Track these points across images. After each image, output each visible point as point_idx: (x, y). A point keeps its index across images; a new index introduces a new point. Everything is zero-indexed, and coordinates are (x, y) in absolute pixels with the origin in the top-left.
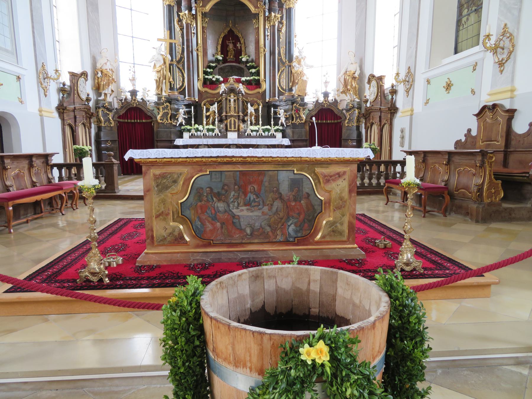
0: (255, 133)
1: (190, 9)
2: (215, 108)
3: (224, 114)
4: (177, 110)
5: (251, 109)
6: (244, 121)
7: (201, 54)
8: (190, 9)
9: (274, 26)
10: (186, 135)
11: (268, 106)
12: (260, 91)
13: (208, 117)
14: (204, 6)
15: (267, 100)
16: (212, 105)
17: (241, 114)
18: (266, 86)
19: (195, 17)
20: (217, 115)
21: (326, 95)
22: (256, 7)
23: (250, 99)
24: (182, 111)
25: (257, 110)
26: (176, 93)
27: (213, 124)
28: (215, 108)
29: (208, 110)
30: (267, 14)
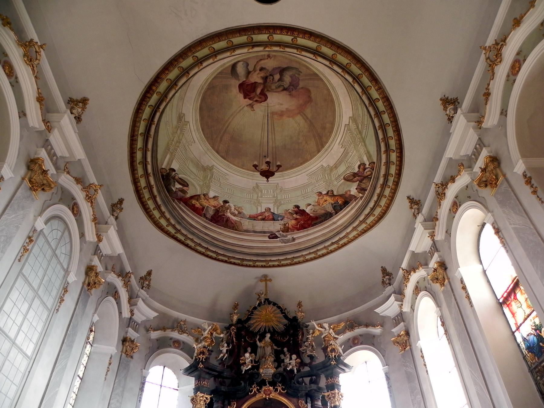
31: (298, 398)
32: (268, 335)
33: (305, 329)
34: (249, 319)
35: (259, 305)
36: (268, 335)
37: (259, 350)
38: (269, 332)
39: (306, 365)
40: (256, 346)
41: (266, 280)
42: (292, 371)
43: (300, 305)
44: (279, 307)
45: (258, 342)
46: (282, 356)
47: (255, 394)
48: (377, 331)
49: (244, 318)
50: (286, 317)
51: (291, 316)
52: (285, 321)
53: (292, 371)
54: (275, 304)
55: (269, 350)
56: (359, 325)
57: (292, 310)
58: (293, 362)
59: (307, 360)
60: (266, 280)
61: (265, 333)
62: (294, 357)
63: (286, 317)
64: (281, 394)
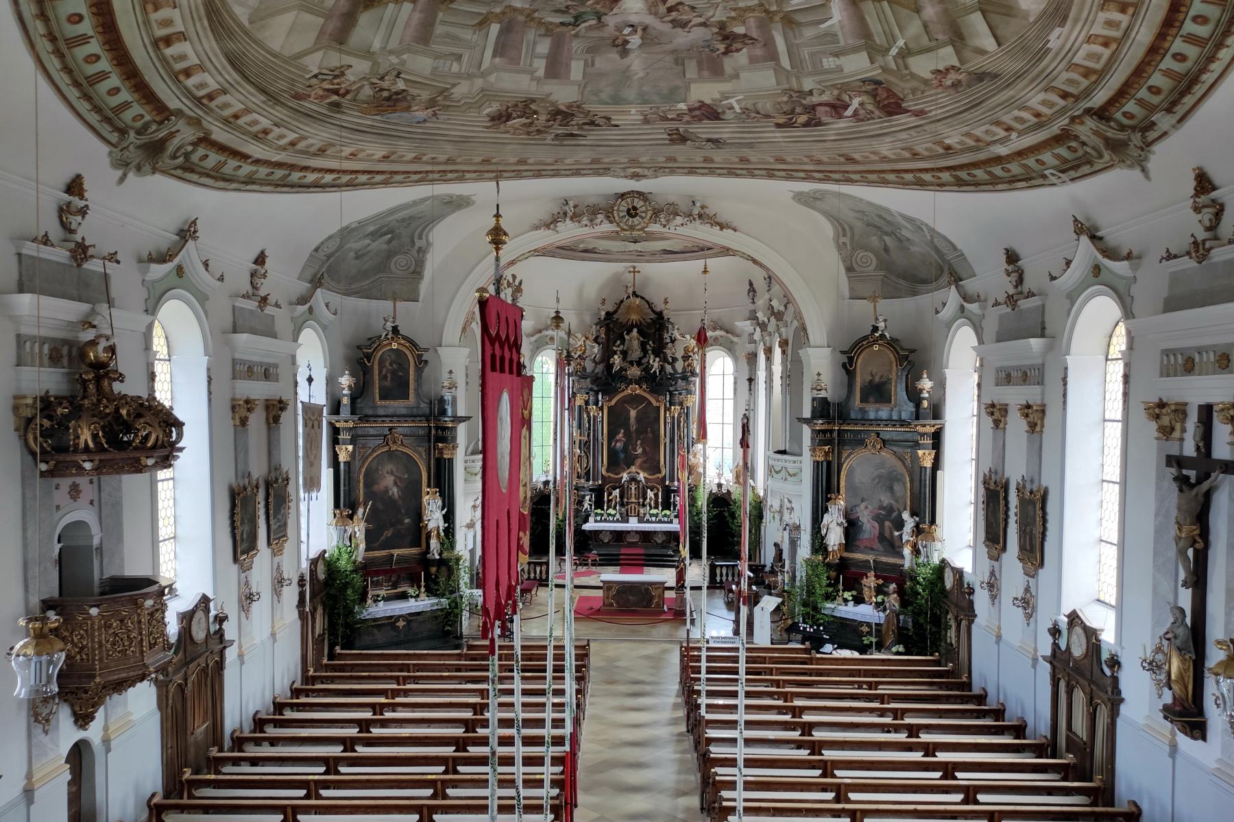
0: (654, 519)
1: (596, 403)
2: (617, 492)
3: (625, 500)
4: (584, 496)
5: (650, 494)
6: (644, 505)
7: (605, 444)
8: (596, 403)
9: (674, 417)
10: (591, 519)
11: (668, 492)
12: (660, 476)
13: (609, 501)
14: (610, 400)
15: (667, 483)
16: (615, 489)
17: (641, 500)
18: (665, 471)
19: (602, 409)
20: (618, 499)
21: (720, 485)
22: (658, 401)
23: (649, 484)
24: (587, 498)
25: (656, 495)
26: (583, 481)
27: (615, 508)
28: (617, 492)
29: (610, 494)
30: (668, 405)
31: (659, 395)
32: (635, 330)
33: (670, 326)
34: (615, 312)
35: (628, 297)
36: (635, 330)
37: (626, 342)
38: (636, 326)
39: (669, 363)
40: (624, 339)
41: (634, 272)
42: (655, 372)
43: (666, 302)
44: (647, 302)
45: (626, 337)
46: (648, 347)
47: (623, 390)
48: (735, 339)
49: (611, 309)
50: (653, 310)
51: (658, 309)
52: (653, 316)
53: (655, 372)
54: (642, 298)
55: (636, 344)
56: (721, 329)
57: (659, 306)
58: (656, 365)
59: (670, 360)
60: (634, 272)
61: (632, 326)
62: (657, 359)
63: (653, 310)
64: (644, 390)
